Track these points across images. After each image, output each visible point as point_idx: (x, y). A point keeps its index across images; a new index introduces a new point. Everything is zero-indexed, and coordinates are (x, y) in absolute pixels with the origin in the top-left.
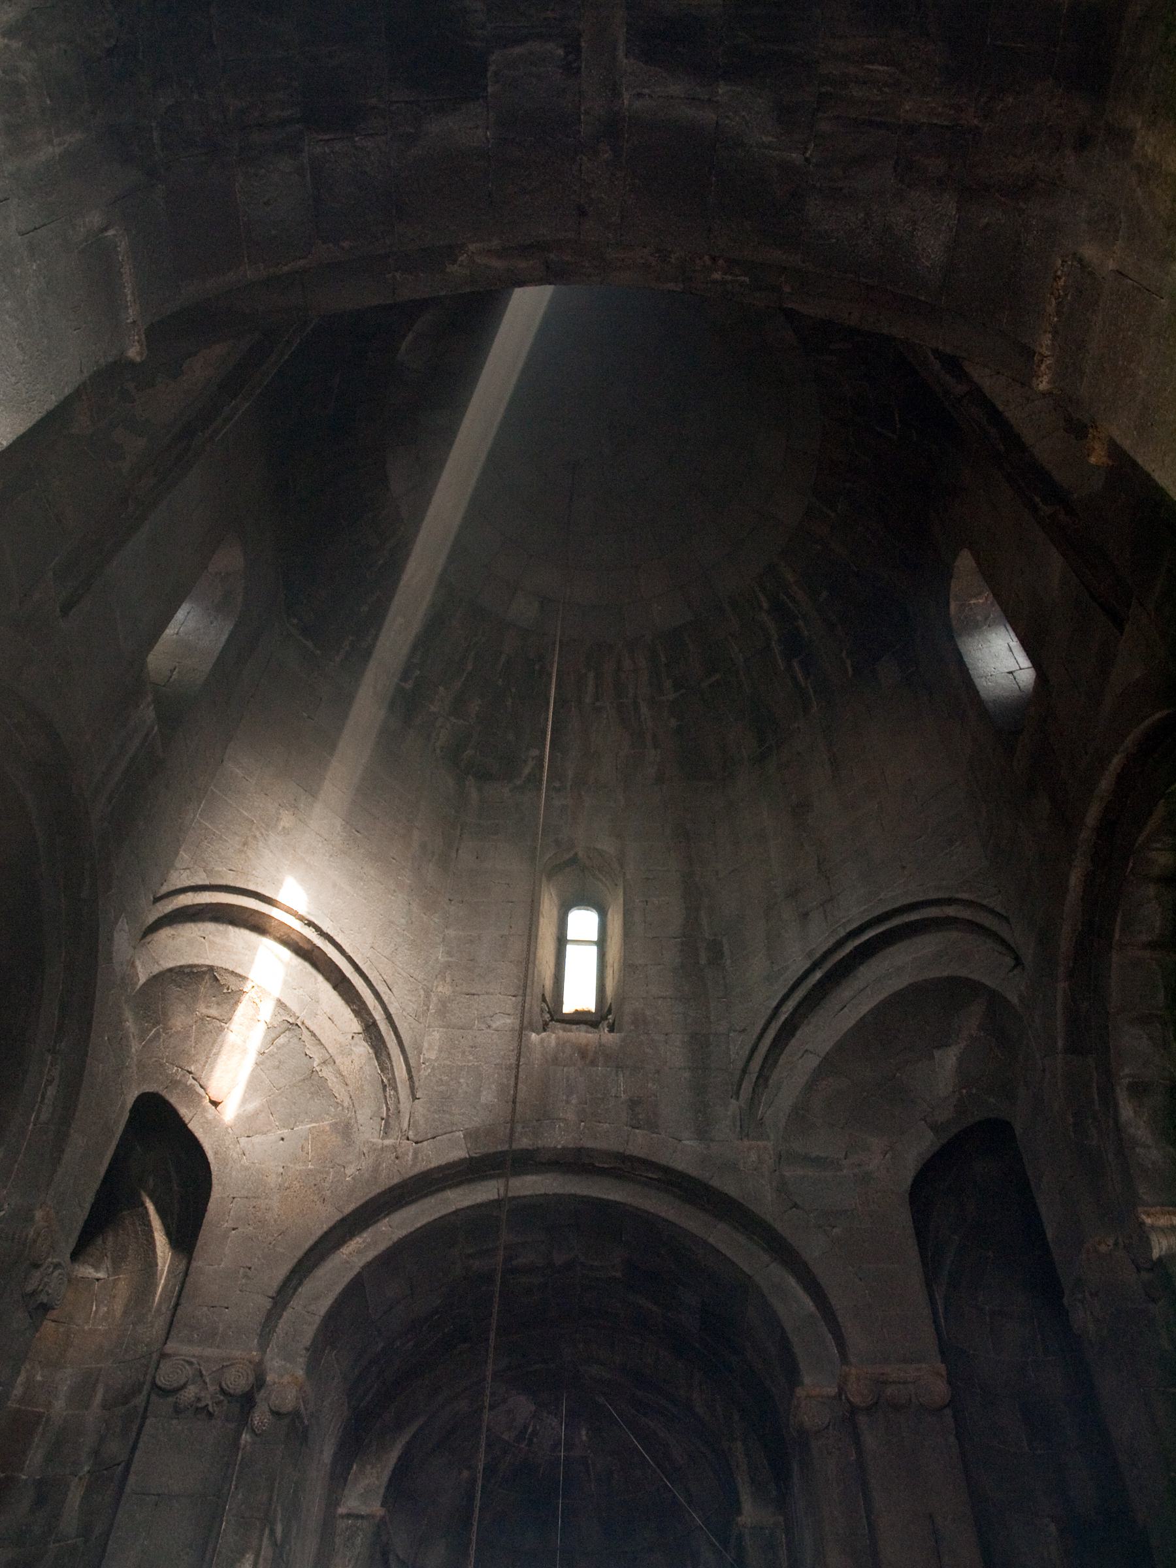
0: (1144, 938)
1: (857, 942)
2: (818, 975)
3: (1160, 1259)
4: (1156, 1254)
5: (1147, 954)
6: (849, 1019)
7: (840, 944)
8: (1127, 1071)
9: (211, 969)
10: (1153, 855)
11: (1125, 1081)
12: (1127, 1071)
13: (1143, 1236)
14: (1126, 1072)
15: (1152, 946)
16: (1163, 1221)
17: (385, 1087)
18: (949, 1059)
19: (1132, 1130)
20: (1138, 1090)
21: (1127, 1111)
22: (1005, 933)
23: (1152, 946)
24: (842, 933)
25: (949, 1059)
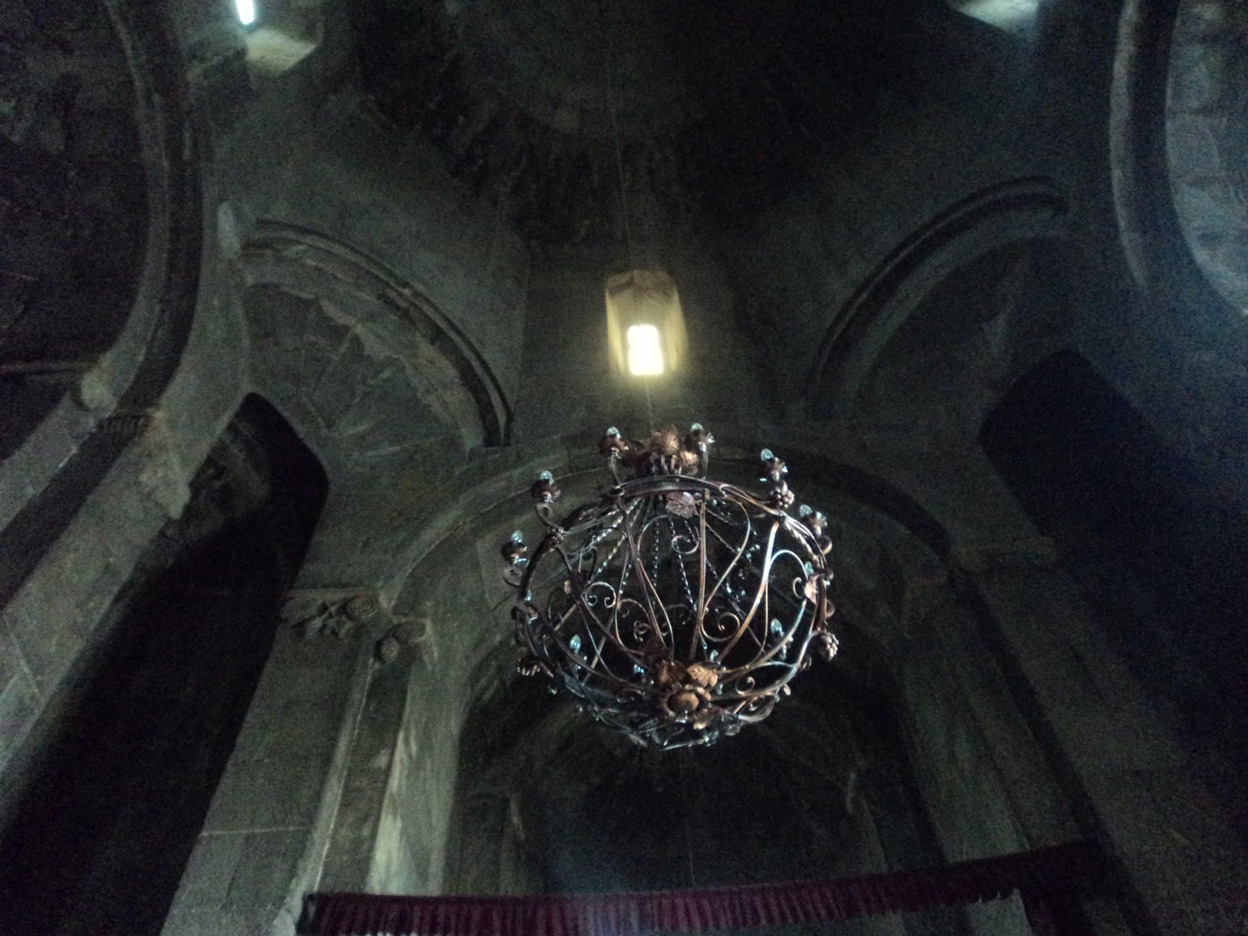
0: (1195, 104)
1: (896, 261)
2: (864, 296)
6: (898, 319)
7: (881, 267)
9: (315, 302)
11: (1195, 233)
12: (1195, 224)
14: (1191, 230)
15: (1205, 110)
17: (483, 417)
18: (998, 329)
20: (1208, 239)
21: (1201, 256)
22: (1041, 188)
23: (1205, 110)
25: (998, 329)
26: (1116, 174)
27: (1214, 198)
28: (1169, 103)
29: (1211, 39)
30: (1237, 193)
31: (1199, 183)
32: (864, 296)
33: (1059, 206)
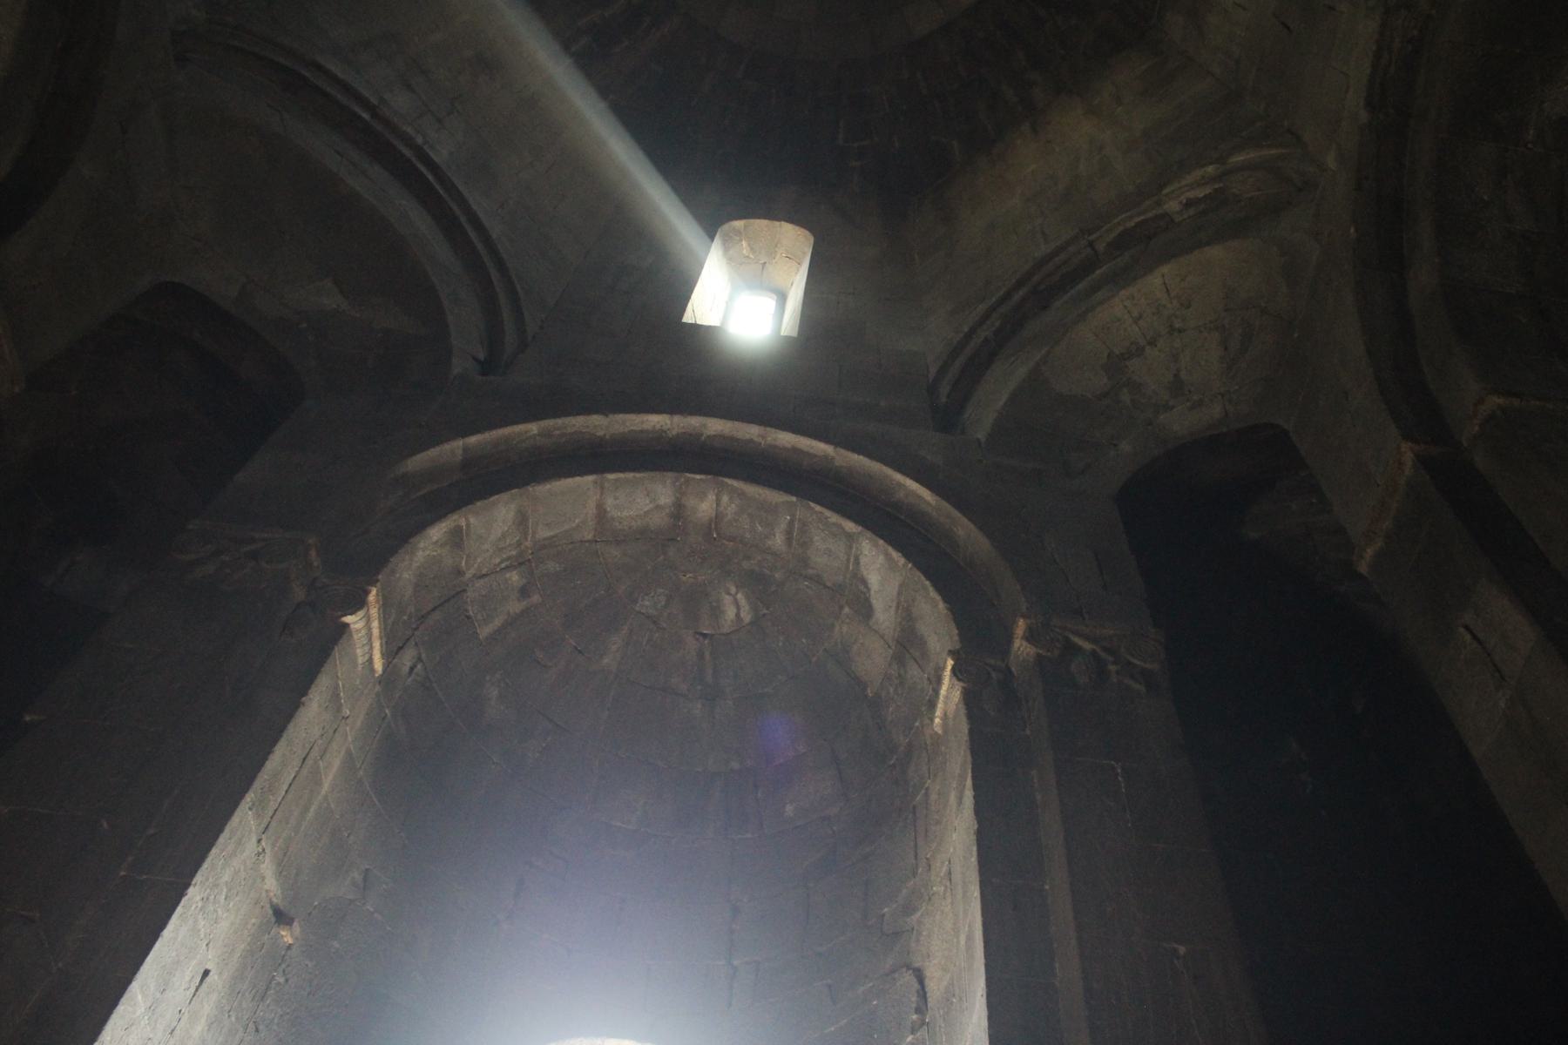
0: (609, 502)
2: (366, 116)
3: (347, 625)
4: (348, 619)
5: (591, 508)
8: (472, 520)
10: (711, 497)
11: (463, 523)
13: (358, 603)
14: (468, 519)
15: (601, 513)
16: (374, 612)
19: (422, 545)
20: (457, 539)
21: (437, 532)
23: (601, 513)
24: (419, 140)
26: (533, 428)
27: (504, 536)
28: (611, 476)
29: (678, 511)
30: (509, 558)
31: (522, 521)
32: (366, 116)
33: (488, 366)
